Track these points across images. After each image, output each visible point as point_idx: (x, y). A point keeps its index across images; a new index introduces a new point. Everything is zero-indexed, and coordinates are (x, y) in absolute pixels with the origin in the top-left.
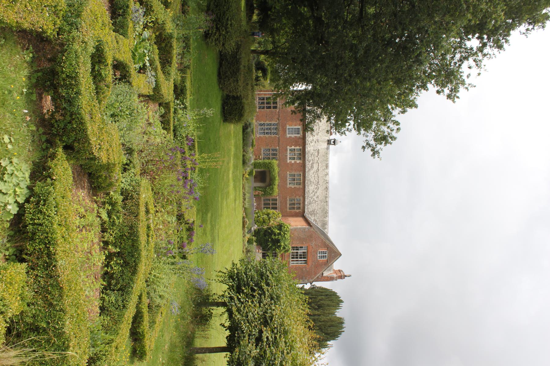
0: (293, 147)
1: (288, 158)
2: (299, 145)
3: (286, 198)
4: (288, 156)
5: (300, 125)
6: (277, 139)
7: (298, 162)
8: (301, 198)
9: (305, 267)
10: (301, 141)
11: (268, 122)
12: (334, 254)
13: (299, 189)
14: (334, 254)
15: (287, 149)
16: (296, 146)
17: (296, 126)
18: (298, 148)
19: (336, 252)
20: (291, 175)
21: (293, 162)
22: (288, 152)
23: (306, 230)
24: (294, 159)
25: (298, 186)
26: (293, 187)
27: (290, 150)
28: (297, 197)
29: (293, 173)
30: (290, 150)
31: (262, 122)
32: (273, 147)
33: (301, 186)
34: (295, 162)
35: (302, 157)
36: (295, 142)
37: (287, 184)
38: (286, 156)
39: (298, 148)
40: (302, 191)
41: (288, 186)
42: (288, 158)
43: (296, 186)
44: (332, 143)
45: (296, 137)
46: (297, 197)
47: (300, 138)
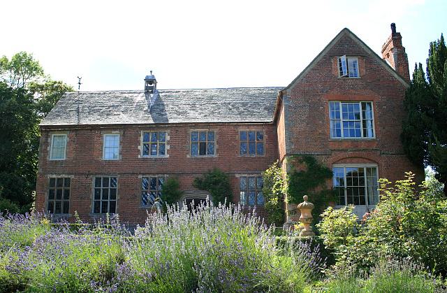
0: (141, 148)
1: (162, 156)
3: (240, 159)
4: (158, 156)
5: (101, 136)
7: (168, 138)
9: (379, 106)
11: (93, 196)
12: (346, 43)
14: (346, 43)
15: (144, 160)
19: (341, 41)
21: (168, 147)
22: (149, 156)
23: (291, 103)
25: (216, 137)
31: (92, 206)
33: (216, 131)
37: (212, 158)
38: (156, 160)
39: (142, 138)
41: (215, 156)
42: (162, 156)
44: (153, 85)
47: (124, 135)
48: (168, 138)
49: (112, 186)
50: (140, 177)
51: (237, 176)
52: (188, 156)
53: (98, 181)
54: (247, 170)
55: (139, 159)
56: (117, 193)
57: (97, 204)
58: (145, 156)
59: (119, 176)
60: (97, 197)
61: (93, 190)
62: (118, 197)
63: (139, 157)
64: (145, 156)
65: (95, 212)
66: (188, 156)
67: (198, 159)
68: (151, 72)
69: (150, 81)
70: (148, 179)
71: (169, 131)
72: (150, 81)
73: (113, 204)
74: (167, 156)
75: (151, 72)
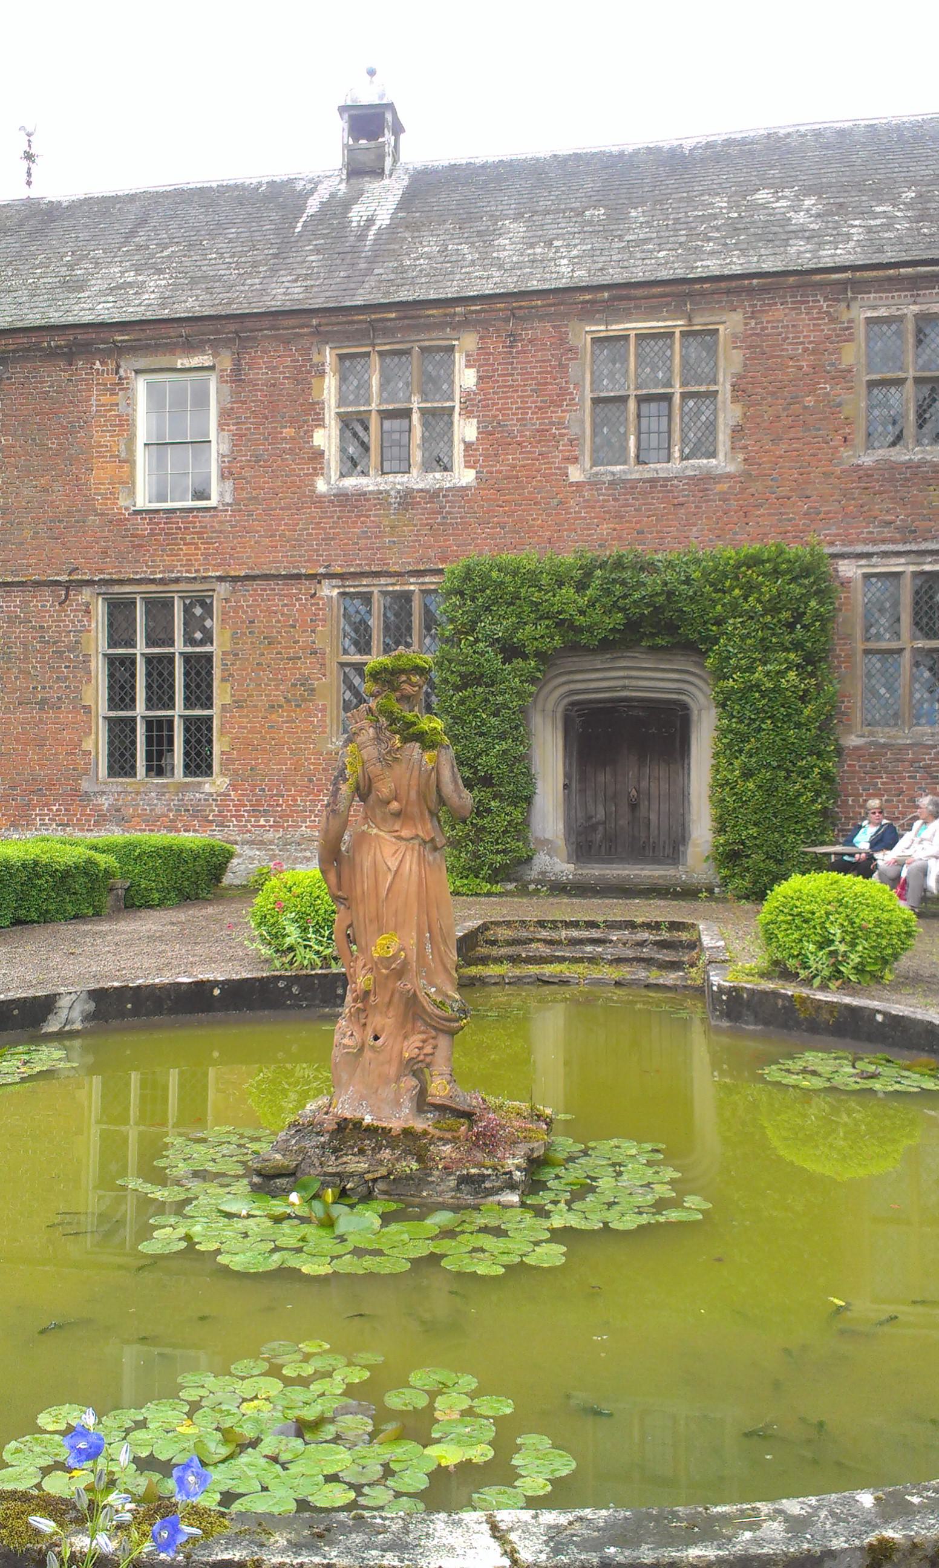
0: (326, 438)
1: (435, 479)
2: (306, 376)
3: (863, 474)
4: (417, 480)
5: (121, 385)
6: (247, 597)
7: (466, 378)
8: (862, 311)
10: (269, 365)
11: (97, 692)
13: (754, 346)
15: (343, 499)
16: (314, 414)
17: (126, 425)
18: (329, 388)
20: (607, 450)
21: (466, 430)
24: (438, 420)
25: (730, 363)
26: (729, 414)
27: (352, 464)
28: (851, 355)
29: (581, 419)
30: (352, 464)
31: (98, 743)
32: (329, 638)
33: (730, 324)
34: (467, 412)
35: (417, 342)
36: (269, 425)
37: (705, 480)
38: (407, 499)
39: (329, 388)
40: (780, 314)
42: (435, 479)
43: (724, 388)
45: (225, 415)
46: (851, 355)
47: (236, 377)
48: (466, 378)
49: (189, 640)
50: (329, 591)
51: (848, 569)
52: (575, 474)
53: (119, 611)
54: (909, 533)
55: (318, 500)
56: (217, 672)
57: (121, 732)
58: (351, 483)
59: (223, 589)
60: (121, 693)
61: (99, 669)
62: (221, 694)
63: (321, 486)
64: (351, 483)
65: (112, 772)
66: (575, 474)
67: (629, 486)
68: (372, 73)
69: (369, 123)
70: (367, 598)
71: (469, 341)
72: (369, 123)
73: (199, 733)
74: (465, 476)
75: (372, 73)
